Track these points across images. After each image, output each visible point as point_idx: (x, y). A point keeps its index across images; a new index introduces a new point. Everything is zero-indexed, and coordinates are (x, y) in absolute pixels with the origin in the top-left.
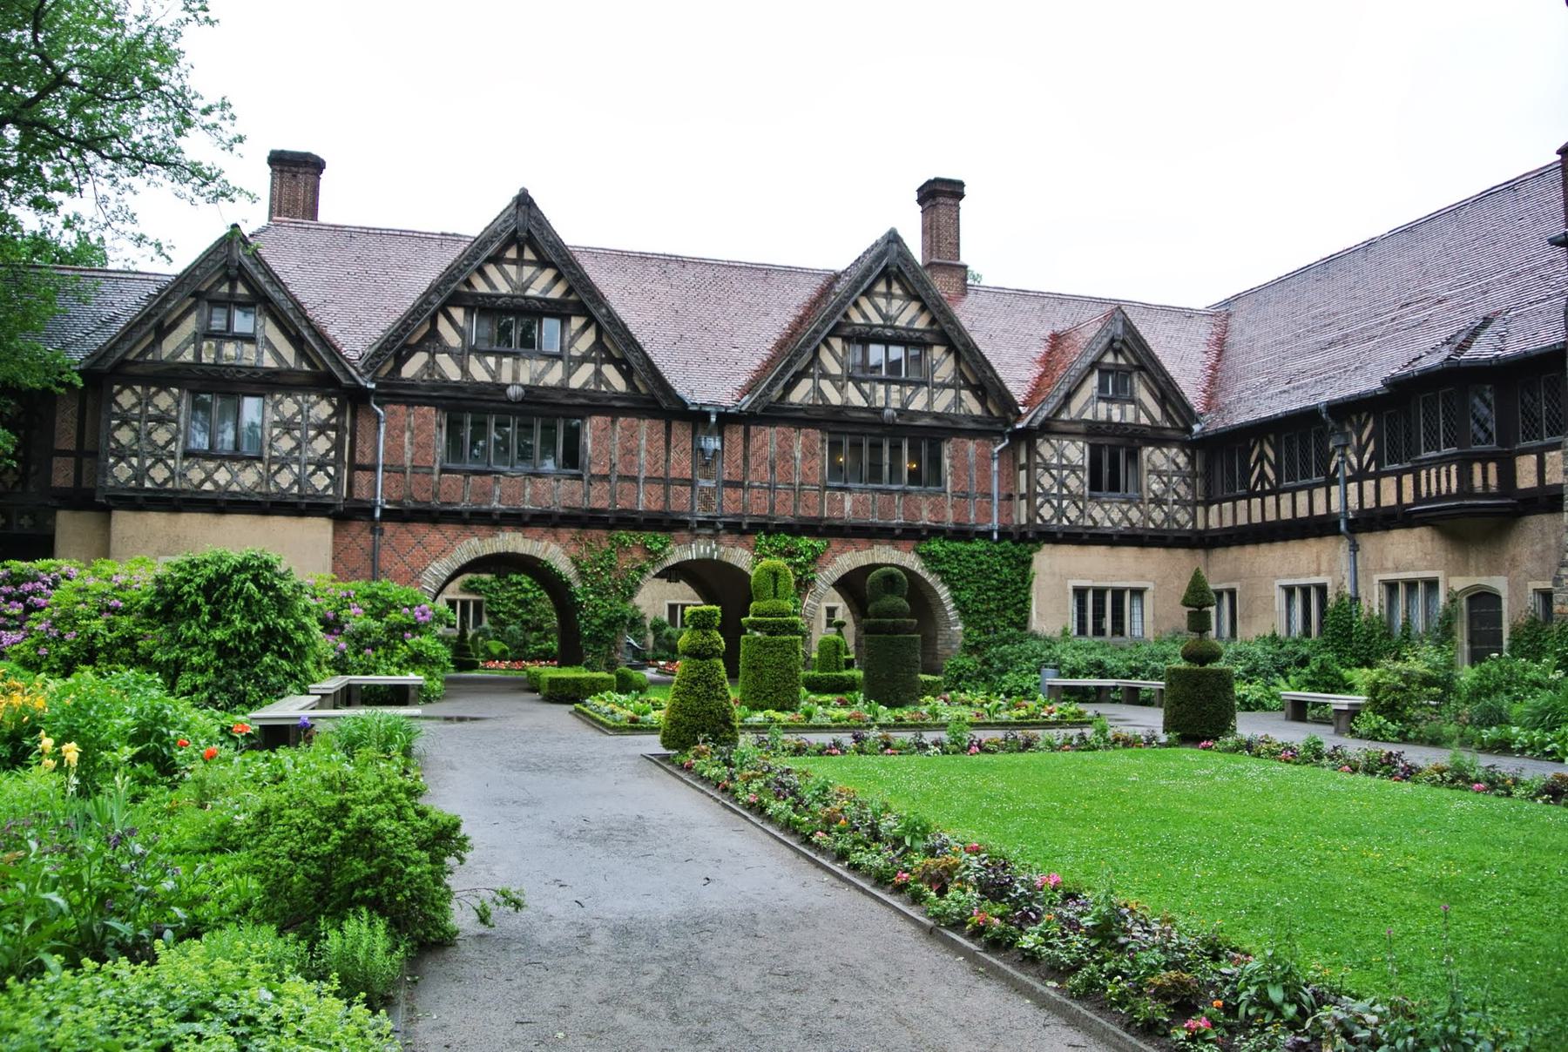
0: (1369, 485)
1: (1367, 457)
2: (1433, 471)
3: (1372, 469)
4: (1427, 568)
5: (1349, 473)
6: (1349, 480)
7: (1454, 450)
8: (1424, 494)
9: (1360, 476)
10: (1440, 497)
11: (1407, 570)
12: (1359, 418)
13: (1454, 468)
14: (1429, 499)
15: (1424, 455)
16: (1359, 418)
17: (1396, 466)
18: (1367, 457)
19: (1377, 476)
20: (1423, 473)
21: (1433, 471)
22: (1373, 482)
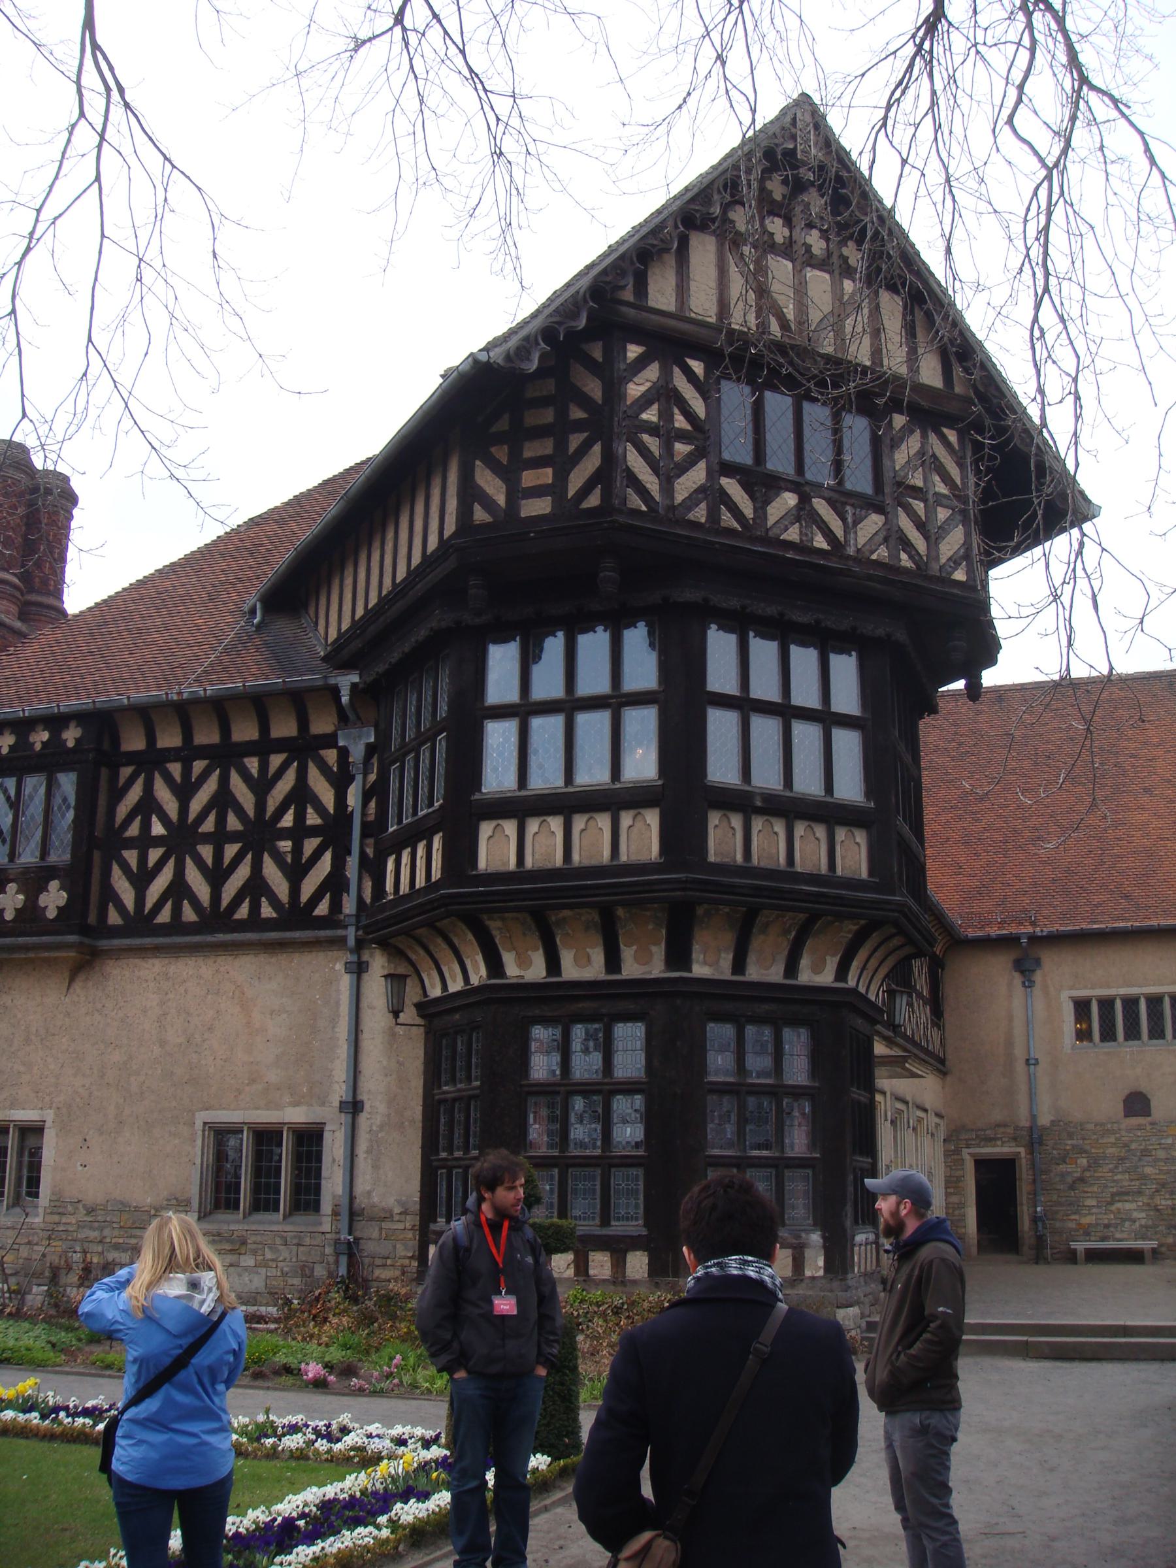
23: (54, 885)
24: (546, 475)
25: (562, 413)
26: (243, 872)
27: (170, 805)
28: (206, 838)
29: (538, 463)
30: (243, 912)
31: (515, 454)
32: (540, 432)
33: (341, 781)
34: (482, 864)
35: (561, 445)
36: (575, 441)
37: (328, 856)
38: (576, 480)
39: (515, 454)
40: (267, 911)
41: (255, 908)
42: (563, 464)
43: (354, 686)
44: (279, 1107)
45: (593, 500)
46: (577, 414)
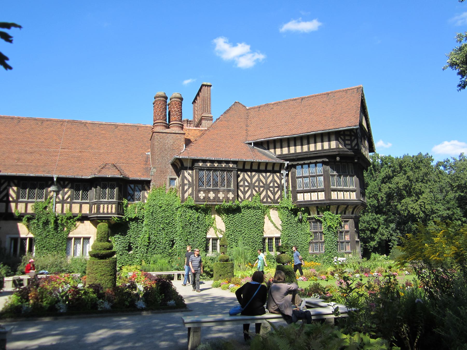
0: (67, 206)
1: (66, 197)
2: (106, 206)
3: (69, 200)
4: (86, 234)
5: (57, 200)
6: (57, 203)
7: (114, 200)
8: (101, 211)
9: (63, 202)
10: (108, 213)
11: (78, 234)
12: (64, 183)
13: (114, 206)
14: (104, 213)
15: (102, 200)
16: (64, 183)
17: (80, 201)
18: (66, 197)
19: (71, 203)
20: (102, 206)
21: (106, 206)
22: (69, 205)
23: (231, 193)
24: (349, 142)
25: (350, 133)
26: (264, 193)
27: (249, 180)
28: (257, 186)
29: (348, 140)
30: (265, 200)
31: (344, 138)
32: (348, 135)
33: (281, 180)
34: (332, 198)
35: (351, 138)
36: (353, 138)
37: (279, 191)
38: (353, 144)
39: (344, 138)
40: (269, 200)
41: (267, 200)
42: (352, 141)
43: (288, 164)
44: (273, 234)
45: (356, 148)
46: (353, 134)
